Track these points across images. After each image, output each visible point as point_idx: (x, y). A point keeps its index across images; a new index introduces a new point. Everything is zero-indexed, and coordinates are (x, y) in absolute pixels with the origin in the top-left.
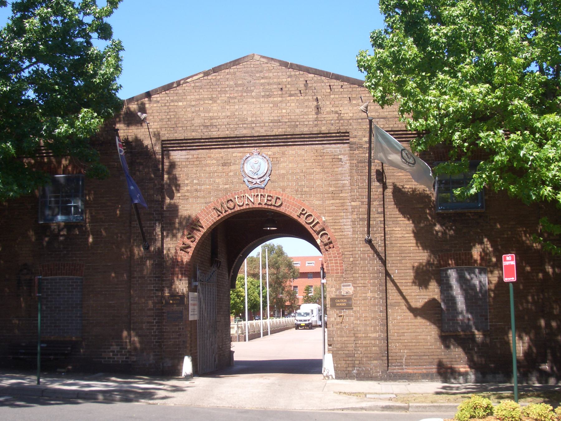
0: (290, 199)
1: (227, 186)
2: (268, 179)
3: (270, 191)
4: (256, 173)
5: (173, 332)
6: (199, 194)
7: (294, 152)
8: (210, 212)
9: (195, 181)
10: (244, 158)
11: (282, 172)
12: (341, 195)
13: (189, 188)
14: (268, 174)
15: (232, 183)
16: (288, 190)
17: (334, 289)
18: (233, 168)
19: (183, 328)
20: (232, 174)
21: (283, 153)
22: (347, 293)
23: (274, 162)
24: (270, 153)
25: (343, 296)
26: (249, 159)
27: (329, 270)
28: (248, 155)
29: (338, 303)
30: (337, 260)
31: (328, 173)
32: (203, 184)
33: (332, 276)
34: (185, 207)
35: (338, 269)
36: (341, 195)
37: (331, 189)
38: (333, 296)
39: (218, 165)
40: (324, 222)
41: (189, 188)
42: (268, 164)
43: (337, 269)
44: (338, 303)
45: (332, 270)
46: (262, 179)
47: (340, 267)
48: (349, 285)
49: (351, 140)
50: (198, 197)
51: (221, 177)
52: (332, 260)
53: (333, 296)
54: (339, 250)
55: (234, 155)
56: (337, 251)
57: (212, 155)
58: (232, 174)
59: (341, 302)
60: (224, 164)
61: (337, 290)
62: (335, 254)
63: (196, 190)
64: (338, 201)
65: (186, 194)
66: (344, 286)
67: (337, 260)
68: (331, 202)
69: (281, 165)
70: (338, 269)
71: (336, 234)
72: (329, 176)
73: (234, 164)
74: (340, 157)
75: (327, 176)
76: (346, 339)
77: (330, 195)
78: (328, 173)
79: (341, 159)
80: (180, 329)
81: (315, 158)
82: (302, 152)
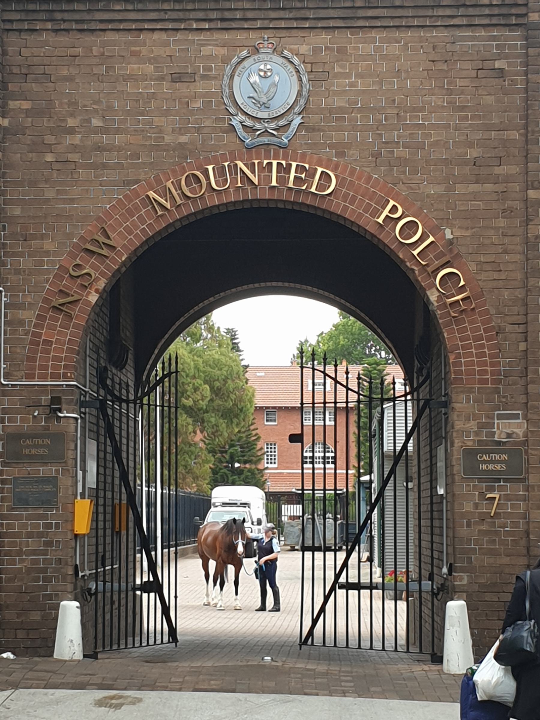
0: (359, 179)
1: (184, 139)
2: (298, 120)
3: (304, 155)
4: (265, 106)
5: (30, 535)
6: (105, 158)
7: (370, 48)
8: (138, 210)
9: (96, 122)
10: (235, 60)
11: (339, 102)
12: (497, 170)
13: (77, 139)
14: (297, 109)
15: (198, 130)
16: (354, 153)
17: (473, 425)
18: (200, 87)
19: (57, 526)
20: (198, 104)
21: (342, 51)
22: (509, 435)
23: (316, 74)
24: (304, 49)
25: (499, 443)
26: (246, 63)
27: (460, 372)
28: (244, 53)
29: (485, 462)
30: (482, 346)
31: (463, 108)
32: (118, 131)
33: (471, 390)
34: (66, 192)
35: (485, 372)
36: (497, 170)
37: (473, 153)
38: (470, 442)
39: (162, 78)
40: (450, 242)
41: (77, 139)
42: (300, 80)
43: (483, 372)
44: (485, 462)
45: (471, 373)
46: (282, 123)
47: (492, 365)
48: (516, 416)
49: (534, 17)
50: (104, 166)
51: (167, 113)
52: (469, 347)
53: (470, 445)
54: (490, 320)
55: (206, 50)
56: (483, 323)
57: (144, 51)
58: (198, 104)
59: (491, 462)
60: (178, 78)
61: (481, 426)
62: (478, 329)
63: (99, 148)
64: (489, 187)
65: (71, 157)
66: (500, 417)
67: (482, 346)
68: (474, 187)
69: (336, 85)
70: (485, 372)
71: (483, 276)
72: (466, 118)
73: (204, 77)
74: (497, 65)
75: (461, 119)
76: (506, 560)
77: (467, 170)
78: (463, 108)
79: (502, 70)
80: (48, 526)
81: (431, 66)
82: (395, 49)
